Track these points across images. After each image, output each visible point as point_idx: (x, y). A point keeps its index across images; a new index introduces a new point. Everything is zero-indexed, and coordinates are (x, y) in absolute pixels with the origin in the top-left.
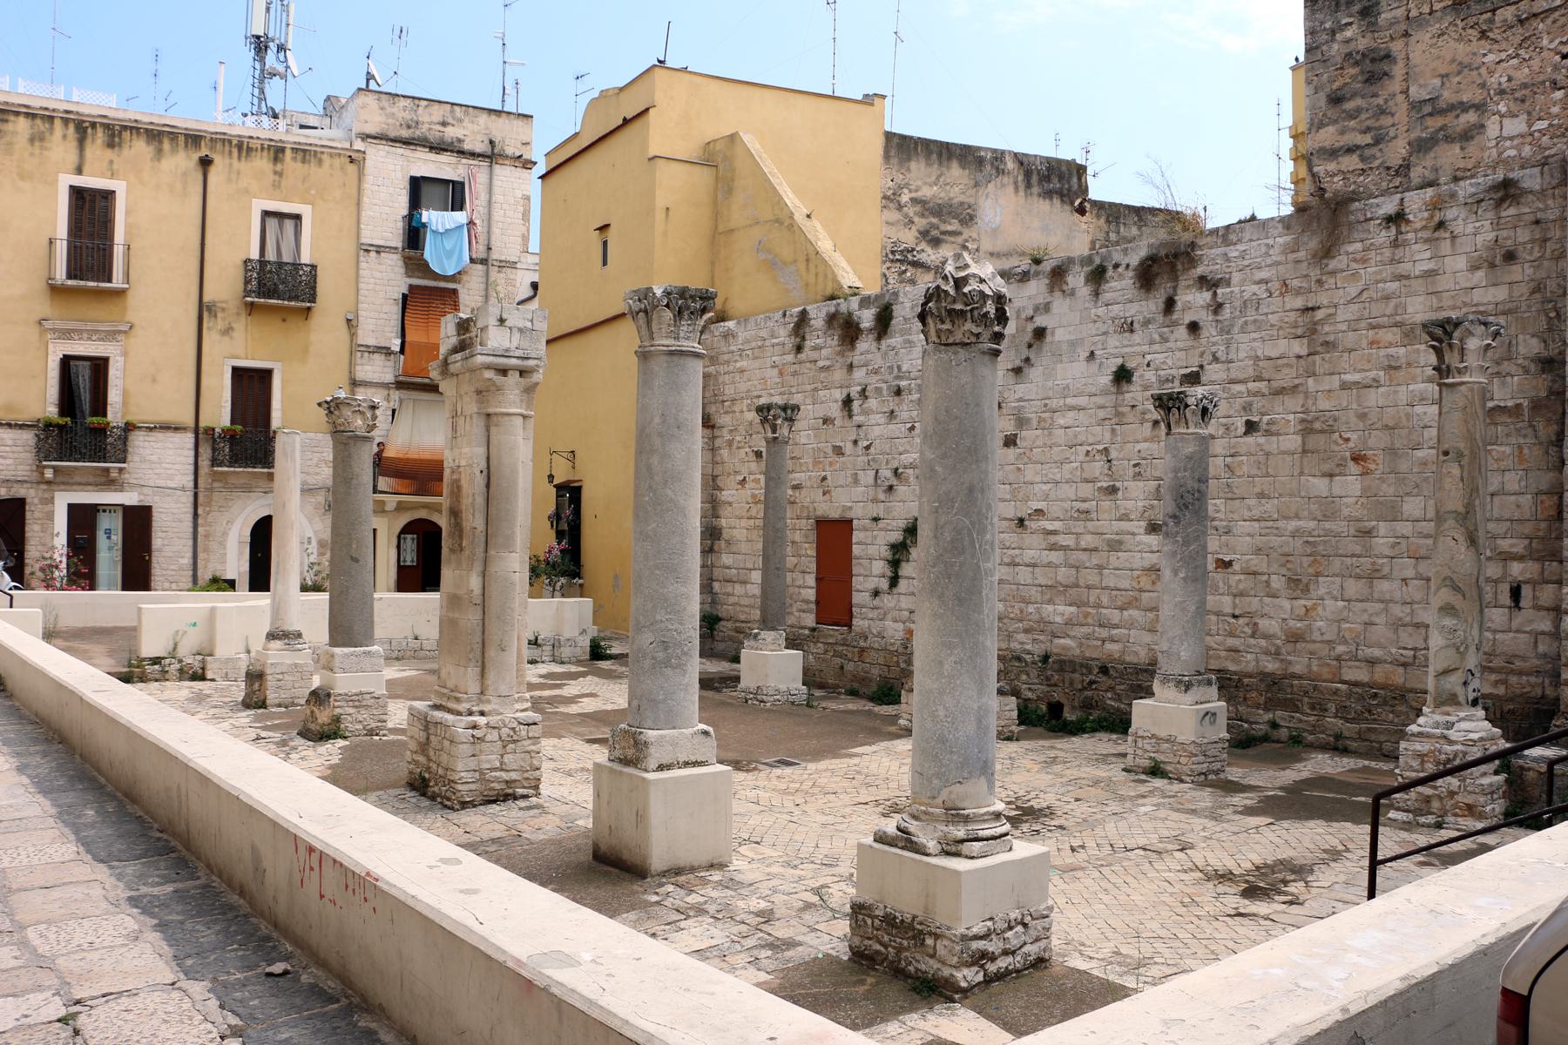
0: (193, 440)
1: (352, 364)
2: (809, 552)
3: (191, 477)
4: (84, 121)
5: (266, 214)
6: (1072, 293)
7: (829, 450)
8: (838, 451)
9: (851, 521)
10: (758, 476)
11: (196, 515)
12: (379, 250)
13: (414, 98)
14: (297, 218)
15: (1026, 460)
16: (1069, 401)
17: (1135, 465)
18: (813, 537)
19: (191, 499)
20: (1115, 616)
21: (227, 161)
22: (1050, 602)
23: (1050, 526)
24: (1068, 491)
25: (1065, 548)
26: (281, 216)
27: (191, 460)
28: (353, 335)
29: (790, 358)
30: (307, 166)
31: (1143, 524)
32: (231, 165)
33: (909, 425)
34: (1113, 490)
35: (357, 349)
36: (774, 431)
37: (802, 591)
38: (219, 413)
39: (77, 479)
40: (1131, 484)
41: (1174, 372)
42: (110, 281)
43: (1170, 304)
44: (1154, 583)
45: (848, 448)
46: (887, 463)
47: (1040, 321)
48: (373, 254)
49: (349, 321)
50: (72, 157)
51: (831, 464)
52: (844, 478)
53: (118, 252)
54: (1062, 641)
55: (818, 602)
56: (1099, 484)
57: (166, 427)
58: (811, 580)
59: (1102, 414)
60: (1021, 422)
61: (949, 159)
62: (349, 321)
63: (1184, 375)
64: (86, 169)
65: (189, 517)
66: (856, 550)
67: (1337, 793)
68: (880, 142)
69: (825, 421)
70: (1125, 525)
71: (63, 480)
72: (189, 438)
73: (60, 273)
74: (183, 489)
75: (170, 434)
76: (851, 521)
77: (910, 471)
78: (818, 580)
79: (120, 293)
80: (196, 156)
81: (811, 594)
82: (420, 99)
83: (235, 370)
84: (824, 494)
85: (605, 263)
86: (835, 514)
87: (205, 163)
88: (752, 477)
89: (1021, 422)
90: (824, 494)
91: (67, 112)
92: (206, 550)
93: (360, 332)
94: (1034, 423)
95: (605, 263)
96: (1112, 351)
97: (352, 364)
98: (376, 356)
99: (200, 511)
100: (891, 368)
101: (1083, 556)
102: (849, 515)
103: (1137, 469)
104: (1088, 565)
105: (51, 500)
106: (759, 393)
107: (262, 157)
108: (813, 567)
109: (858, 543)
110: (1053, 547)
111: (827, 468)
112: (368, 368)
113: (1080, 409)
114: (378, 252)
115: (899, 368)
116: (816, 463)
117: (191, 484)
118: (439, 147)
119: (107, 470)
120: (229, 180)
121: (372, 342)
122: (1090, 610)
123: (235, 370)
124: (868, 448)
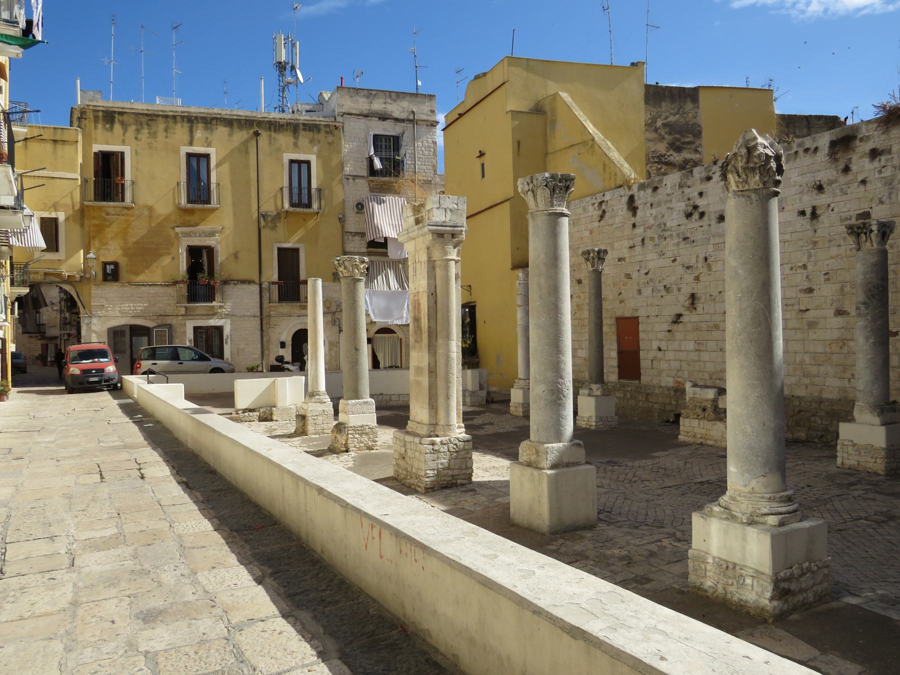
0: (259, 289)
1: (343, 243)
3: (259, 310)
4: (192, 117)
5: (292, 162)
8: (628, 276)
9: (638, 317)
10: (580, 294)
11: (262, 330)
12: (355, 177)
13: (368, 90)
14: (308, 163)
17: (825, 274)
19: (259, 322)
20: (814, 370)
21: (268, 133)
26: (299, 162)
27: (258, 300)
28: (343, 227)
29: (596, 224)
30: (311, 133)
32: (270, 136)
33: (673, 258)
34: (810, 290)
35: (344, 233)
36: (593, 266)
38: (272, 273)
39: (198, 313)
41: (851, 213)
42: (210, 204)
43: (847, 170)
44: (841, 348)
45: (635, 275)
46: (659, 282)
48: (351, 180)
49: (340, 219)
50: (186, 138)
53: (213, 186)
55: (619, 366)
56: (800, 288)
57: (244, 282)
59: (801, 243)
61: (686, 97)
62: (340, 219)
63: (858, 215)
64: (195, 142)
65: (259, 332)
66: (641, 335)
68: (642, 92)
69: (620, 260)
71: (188, 314)
72: (255, 288)
73: (183, 201)
74: (255, 316)
75: (245, 286)
76: (638, 317)
79: (213, 210)
80: (251, 132)
82: (372, 90)
83: (279, 249)
84: (621, 303)
85: (483, 176)
86: (628, 314)
87: (257, 134)
90: (621, 303)
91: (182, 112)
92: (268, 349)
93: (346, 225)
95: (483, 176)
97: (343, 243)
98: (356, 238)
99: (264, 328)
100: (659, 225)
102: (636, 315)
103: (827, 277)
105: (185, 325)
107: (287, 130)
109: (643, 331)
111: (622, 287)
112: (351, 245)
114: (354, 179)
115: (665, 224)
117: (259, 314)
118: (383, 117)
119: (213, 307)
120: (270, 143)
121: (353, 230)
123: (279, 249)
124: (647, 274)
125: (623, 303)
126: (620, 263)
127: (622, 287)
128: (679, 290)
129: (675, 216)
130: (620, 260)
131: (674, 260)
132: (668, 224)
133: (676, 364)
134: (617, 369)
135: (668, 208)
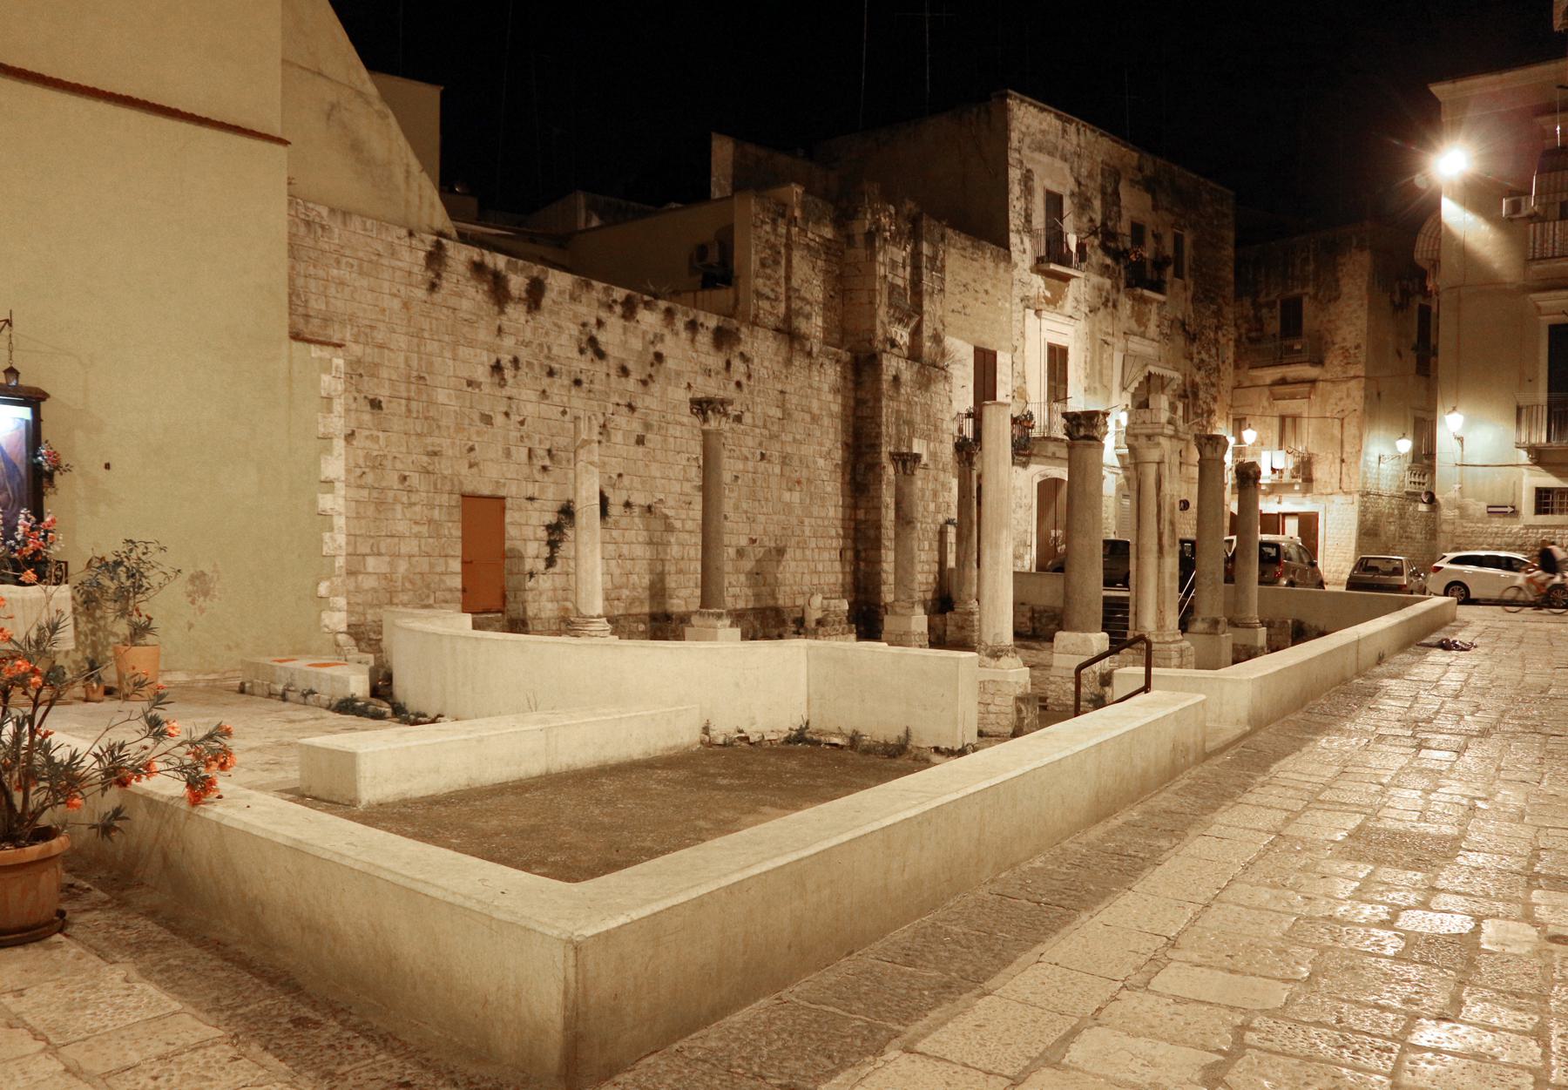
6: (677, 334)
7: (476, 417)
9: (503, 498)
18: (457, 515)
47: (659, 347)
51: (478, 433)
52: (496, 451)
55: (464, 590)
58: (456, 566)
60: (647, 426)
67: (1462, 571)
69: (470, 383)
77: (562, 454)
78: (465, 563)
81: (457, 582)
84: (471, 466)
89: (647, 426)
90: (471, 466)
94: (656, 428)
100: (541, 345)
101: (687, 536)
102: (501, 493)
109: (512, 523)
111: (474, 438)
113: (682, 425)
115: (549, 349)
116: (459, 428)
124: (522, 423)
125: (475, 470)
126: (470, 389)
127: (474, 438)
129: (564, 339)
130: (470, 383)
131: (564, 413)
132: (555, 350)
134: (459, 595)
135: (556, 325)
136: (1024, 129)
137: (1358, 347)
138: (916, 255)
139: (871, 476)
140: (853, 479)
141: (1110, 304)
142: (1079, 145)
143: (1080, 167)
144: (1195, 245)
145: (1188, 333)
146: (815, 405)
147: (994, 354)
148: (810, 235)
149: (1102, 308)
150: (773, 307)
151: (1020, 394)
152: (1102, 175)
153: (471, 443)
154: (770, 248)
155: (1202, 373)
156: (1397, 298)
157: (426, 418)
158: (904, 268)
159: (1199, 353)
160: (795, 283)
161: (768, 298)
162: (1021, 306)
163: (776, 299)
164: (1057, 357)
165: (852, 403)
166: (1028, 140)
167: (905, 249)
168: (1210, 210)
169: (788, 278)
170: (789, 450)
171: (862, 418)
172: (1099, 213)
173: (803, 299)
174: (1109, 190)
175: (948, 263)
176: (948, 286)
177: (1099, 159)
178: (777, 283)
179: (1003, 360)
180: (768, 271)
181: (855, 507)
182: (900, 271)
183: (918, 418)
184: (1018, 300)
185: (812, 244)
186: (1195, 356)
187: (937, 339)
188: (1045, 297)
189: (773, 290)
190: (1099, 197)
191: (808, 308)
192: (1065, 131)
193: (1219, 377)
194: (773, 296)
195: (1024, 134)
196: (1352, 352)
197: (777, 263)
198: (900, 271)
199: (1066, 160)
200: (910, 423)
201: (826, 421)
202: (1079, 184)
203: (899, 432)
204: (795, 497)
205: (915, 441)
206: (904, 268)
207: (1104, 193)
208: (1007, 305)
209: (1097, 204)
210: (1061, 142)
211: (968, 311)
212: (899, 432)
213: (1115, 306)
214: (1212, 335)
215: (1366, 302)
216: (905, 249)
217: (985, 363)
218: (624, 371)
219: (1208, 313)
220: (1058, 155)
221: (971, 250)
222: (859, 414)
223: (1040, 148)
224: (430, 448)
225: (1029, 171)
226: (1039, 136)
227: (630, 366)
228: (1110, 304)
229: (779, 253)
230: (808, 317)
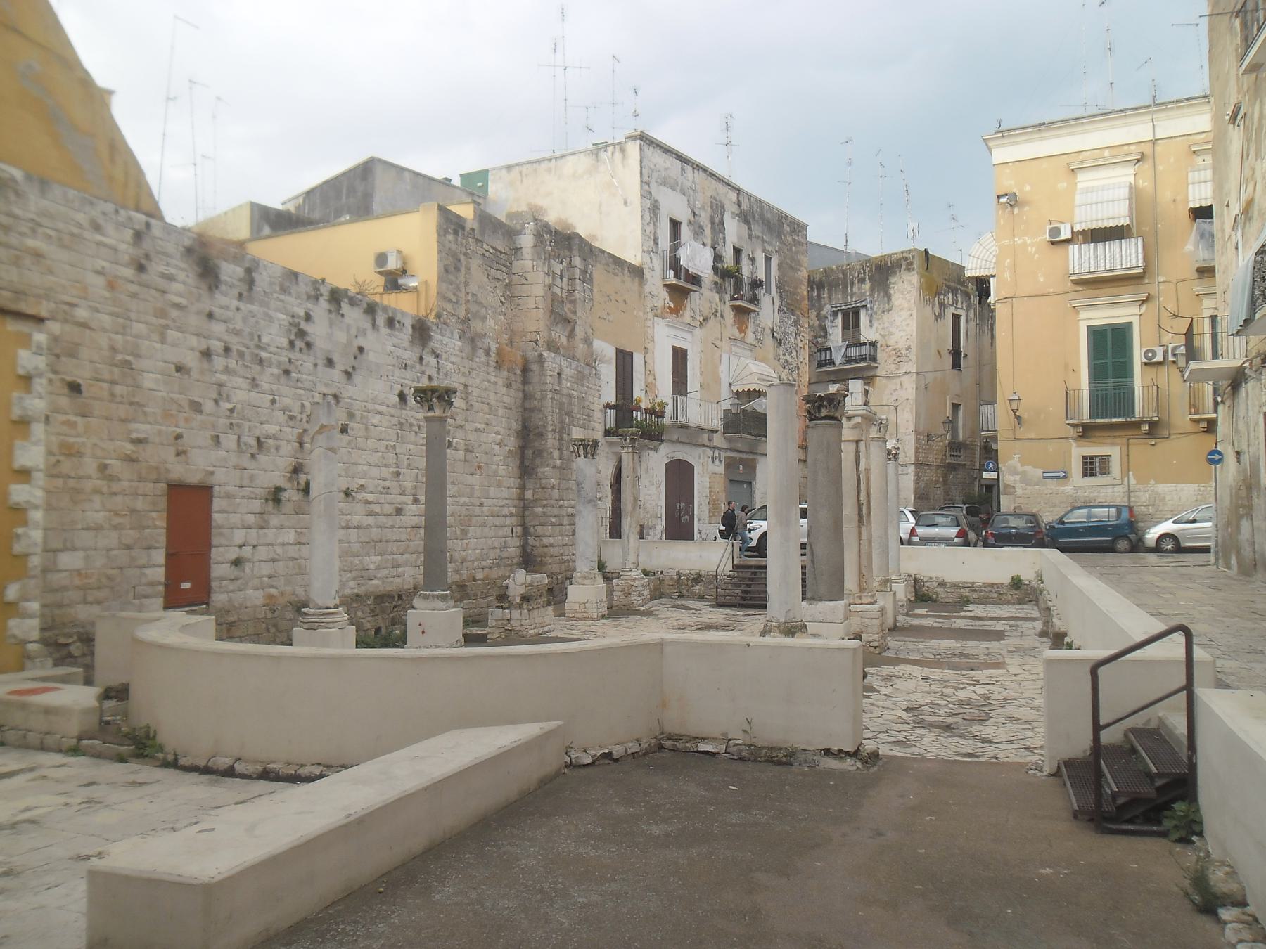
2: (158, 523)
7: (185, 404)
9: (210, 488)
15: (353, 446)
16: (377, 407)
17: (408, 459)
18: (163, 503)
22: (368, 554)
23: (370, 497)
24: (375, 472)
25: (377, 514)
31: (411, 498)
37: (147, 571)
40: (405, 470)
45: (209, 406)
47: (361, 342)
51: (187, 420)
52: (204, 438)
54: (373, 582)
58: (159, 557)
60: (351, 416)
66: (217, 518)
70: (403, 498)
76: (210, 488)
77: (271, 441)
78: (169, 556)
84: (178, 454)
86: (194, 478)
88: (62, 418)
89: (351, 416)
90: (178, 454)
96: (397, 379)
102: (210, 481)
104: (387, 525)
106: (74, 300)
108: (162, 540)
110: (370, 514)
111: (182, 423)
113: (381, 414)
122: (388, 557)
125: (182, 458)
126: (178, 375)
128: (277, 448)
129: (274, 329)
130: (179, 369)
132: (265, 339)
133: (266, 569)
136: (652, 166)
137: (909, 348)
138: (571, 266)
139: (538, 461)
140: (522, 462)
141: (718, 314)
142: (694, 182)
143: (695, 201)
144: (780, 266)
145: (777, 339)
146: (492, 397)
147: (631, 355)
148: (485, 246)
149: (713, 317)
150: (454, 309)
151: (649, 388)
152: (712, 207)
153: (178, 430)
154: (452, 256)
155: (787, 370)
156: (937, 310)
157: (131, 404)
158: (561, 278)
159: (784, 355)
160: (473, 288)
161: (450, 301)
162: (650, 316)
163: (457, 302)
164: (679, 357)
165: (520, 395)
166: (655, 175)
167: (561, 263)
168: (790, 239)
169: (467, 284)
170: (470, 437)
171: (532, 410)
172: (710, 239)
173: (479, 303)
174: (717, 221)
175: (595, 275)
176: (596, 295)
177: (709, 195)
178: (458, 288)
179: (638, 360)
180: (451, 277)
181: (523, 488)
182: (558, 282)
183: (576, 409)
184: (649, 310)
185: (487, 254)
186: (781, 357)
187: (587, 341)
188: (669, 307)
189: (454, 294)
190: (709, 225)
191: (483, 311)
192: (683, 170)
193: (798, 374)
194: (454, 300)
195: (652, 171)
196: (904, 352)
197: (457, 269)
198: (558, 282)
199: (684, 195)
200: (569, 413)
201: (501, 412)
202: (695, 214)
203: (562, 422)
204: (475, 480)
205: (574, 429)
206: (561, 278)
207: (713, 223)
208: (641, 314)
209: (708, 230)
210: (680, 179)
211: (611, 318)
212: (562, 422)
213: (722, 316)
214: (793, 341)
215: (914, 313)
216: (561, 263)
217: (624, 361)
218: (330, 363)
219: (790, 322)
220: (678, 189)
221: (613, 266)
222: (527, 405)
223: (664, 183)
224: (134, 436)
225: (656, 201)
226: (663, 174)
227: (336, 358)
228: (718, 314)
229: (460, 261)
230: (483, 319)
